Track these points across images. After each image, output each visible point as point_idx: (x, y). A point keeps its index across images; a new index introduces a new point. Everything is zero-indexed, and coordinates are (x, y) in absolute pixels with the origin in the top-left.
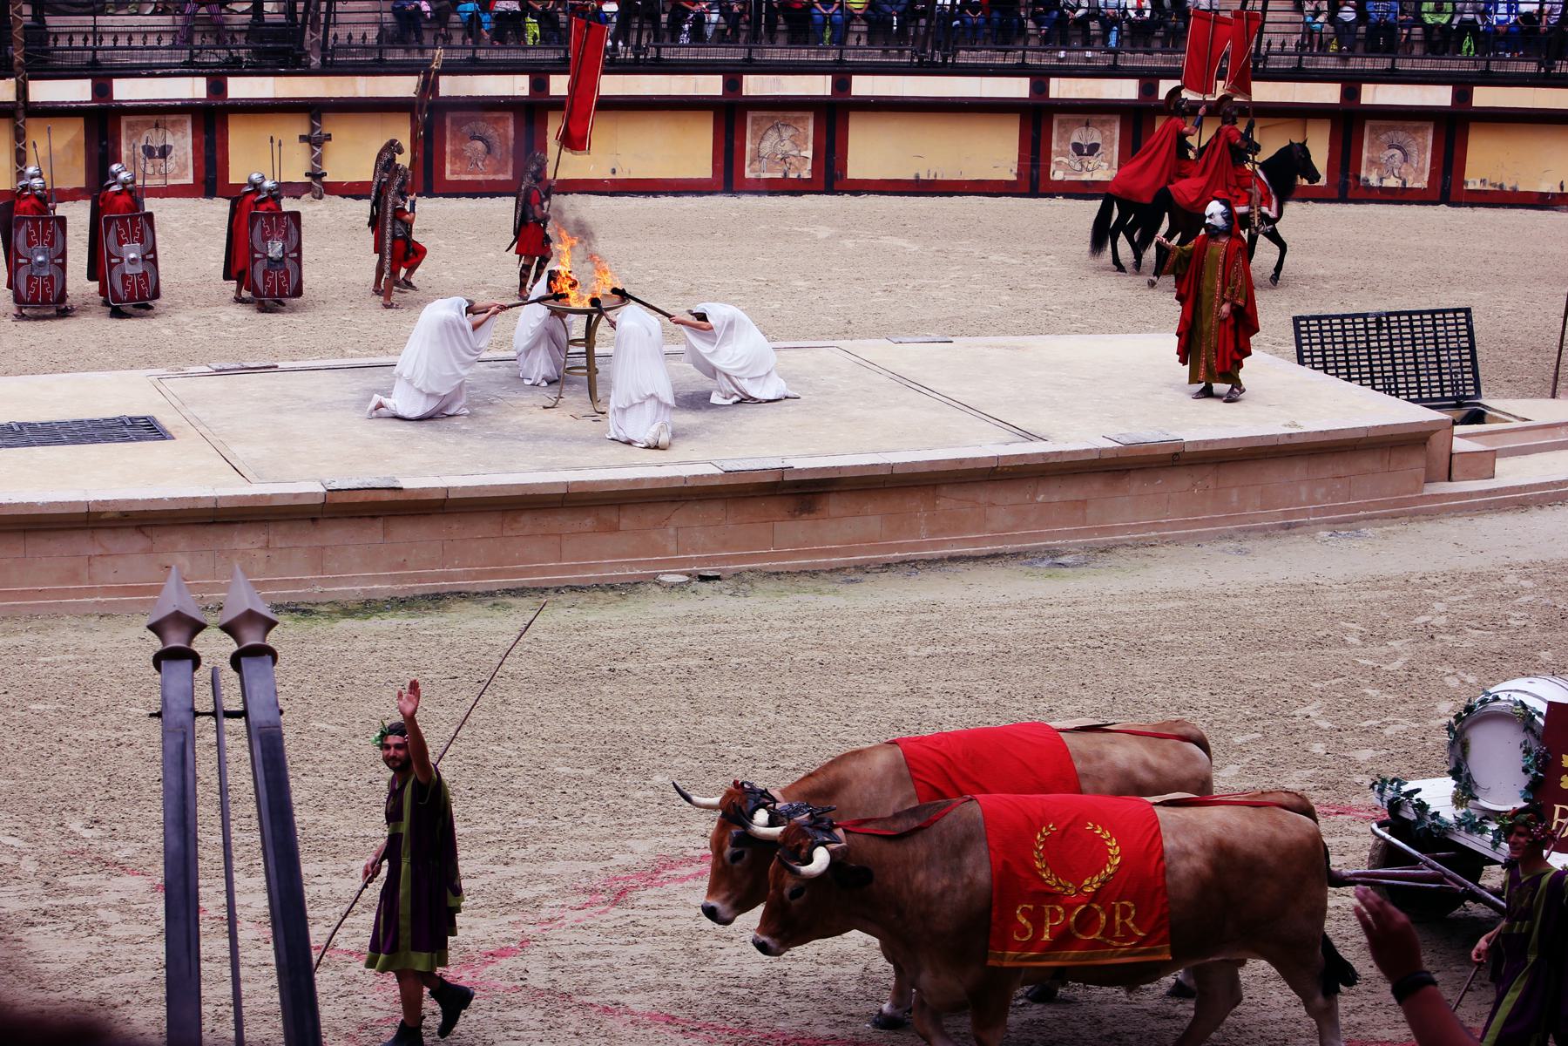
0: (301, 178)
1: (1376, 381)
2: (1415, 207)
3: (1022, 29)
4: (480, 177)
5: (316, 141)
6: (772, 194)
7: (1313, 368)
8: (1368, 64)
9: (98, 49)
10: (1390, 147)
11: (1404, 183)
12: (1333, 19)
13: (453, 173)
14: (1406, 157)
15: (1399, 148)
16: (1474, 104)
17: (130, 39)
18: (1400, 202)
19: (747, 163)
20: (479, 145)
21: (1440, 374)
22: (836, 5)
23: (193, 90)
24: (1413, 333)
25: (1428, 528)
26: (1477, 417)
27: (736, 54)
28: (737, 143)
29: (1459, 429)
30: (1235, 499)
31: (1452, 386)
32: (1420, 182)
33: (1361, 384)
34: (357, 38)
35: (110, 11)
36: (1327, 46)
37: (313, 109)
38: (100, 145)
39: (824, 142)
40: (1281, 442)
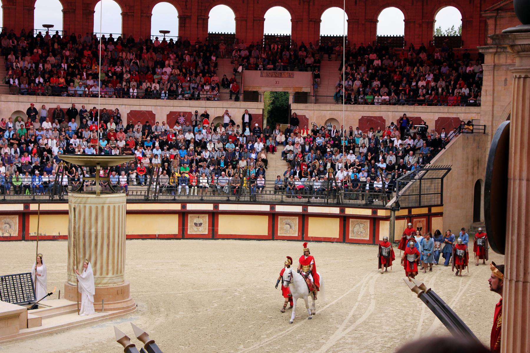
2: (14, 242)
10: (5, 223)
11: (10, 235)
14: (10, 226)
15: (8, 224)
18: (10, 241)
21: (23, 294)
24: (13, 282)
25: (22, 344)
26: (36, 307)
29: (29, 311)
31: (27, 298)
32: (15, 234)
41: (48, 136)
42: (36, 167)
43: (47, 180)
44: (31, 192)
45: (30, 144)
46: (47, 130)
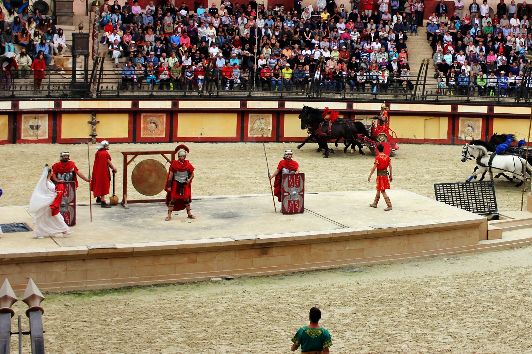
0: (87, 136)
1: (463, 206)
3: (344, 87)
4: (153, 136)
5: (93, 123)
6: (257, 142)
7: (441, 202)
8: (460, 99)
9: (14, 91)
10: (468, 126)
12: (447, 84)
13: (143, 135)
14: (473, 129)
15: (471, 127)
16: (495, 112)
17: (26, 87)
19: (249, 131)
20: (153, 125)
22: (280, 78)
23: (49, 105)
25: (481, 256)
26: (496, 218)
27: (245, 94)
28: (245, 125)
29: (490, 222)
30: (415, 247)
33: (458, 207)
34: (110, 88)
35: (20, 77)
36: (446, 93)
37: (94, 112)
38: (14, 125)
39: (276, 124)
40: (430, 227)
41: (516, 34)
42: (502, 68)
43: (513, 81)
44: (496, 93)
45: (496, 42)
46: (515, 27)
